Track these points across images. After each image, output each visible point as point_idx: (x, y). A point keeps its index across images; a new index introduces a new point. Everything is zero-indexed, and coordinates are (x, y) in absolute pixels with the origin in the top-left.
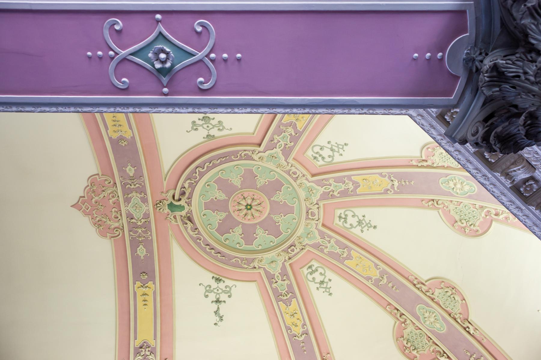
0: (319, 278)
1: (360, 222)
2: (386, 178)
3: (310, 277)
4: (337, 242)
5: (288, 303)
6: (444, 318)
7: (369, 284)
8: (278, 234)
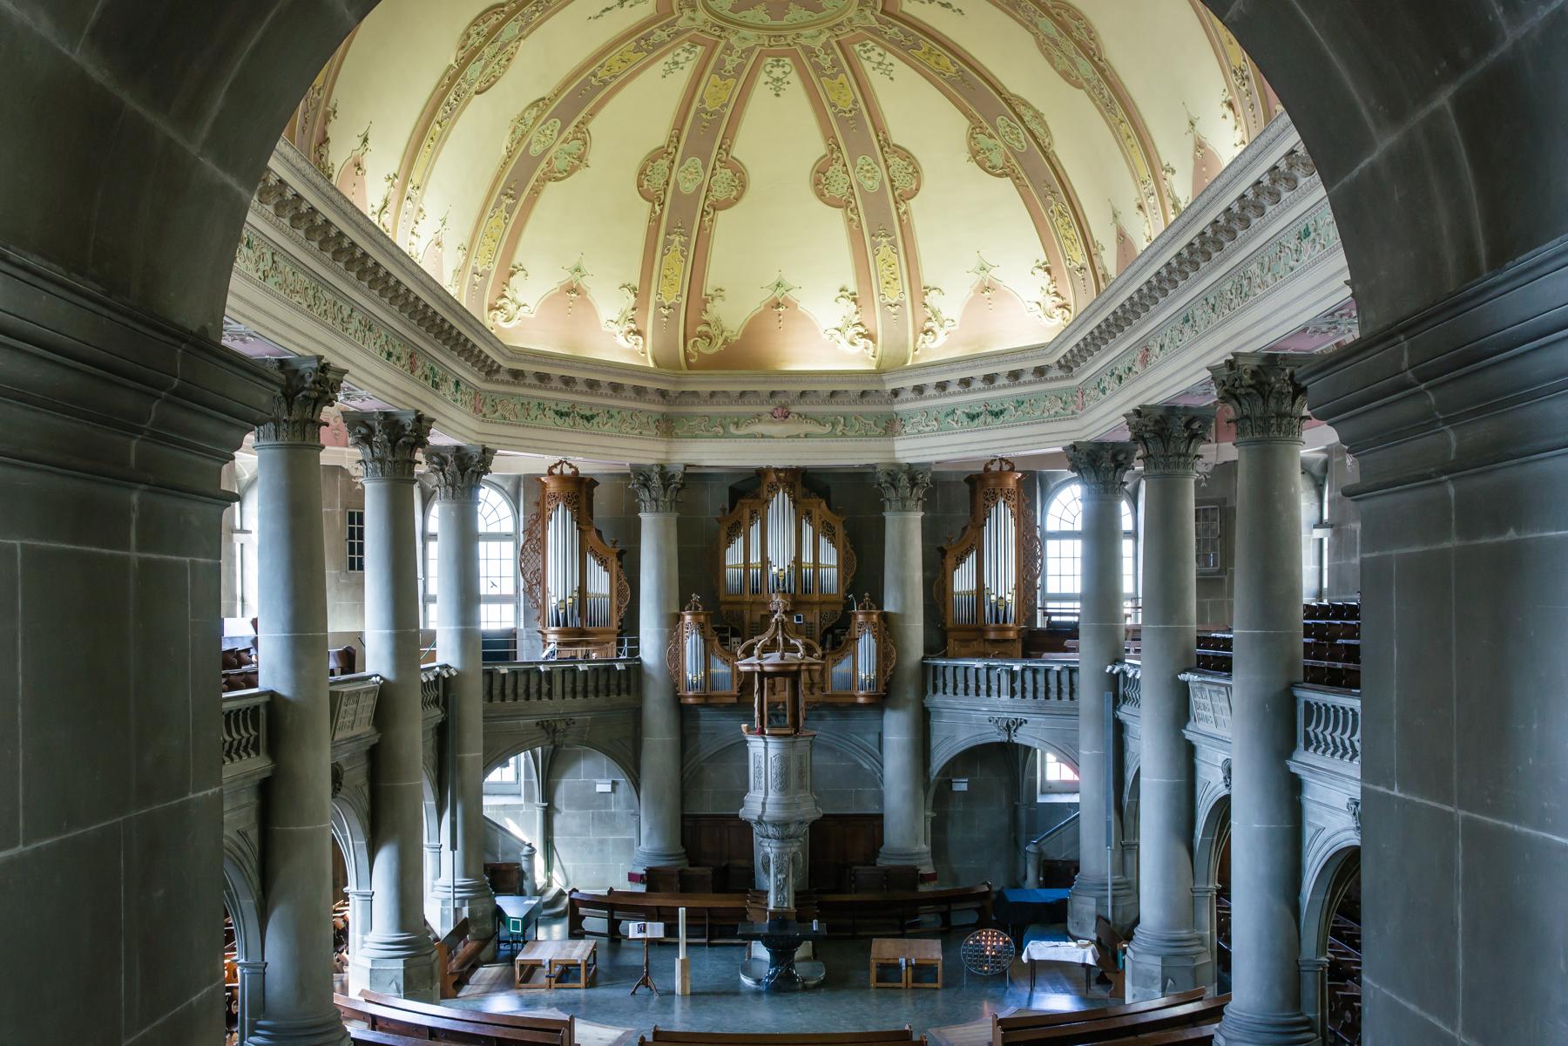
0: (681, 59)
1: (778, 80)
5: (638, 49)
6: (700, 187)
7: (696, 104)
8: (734, 10)
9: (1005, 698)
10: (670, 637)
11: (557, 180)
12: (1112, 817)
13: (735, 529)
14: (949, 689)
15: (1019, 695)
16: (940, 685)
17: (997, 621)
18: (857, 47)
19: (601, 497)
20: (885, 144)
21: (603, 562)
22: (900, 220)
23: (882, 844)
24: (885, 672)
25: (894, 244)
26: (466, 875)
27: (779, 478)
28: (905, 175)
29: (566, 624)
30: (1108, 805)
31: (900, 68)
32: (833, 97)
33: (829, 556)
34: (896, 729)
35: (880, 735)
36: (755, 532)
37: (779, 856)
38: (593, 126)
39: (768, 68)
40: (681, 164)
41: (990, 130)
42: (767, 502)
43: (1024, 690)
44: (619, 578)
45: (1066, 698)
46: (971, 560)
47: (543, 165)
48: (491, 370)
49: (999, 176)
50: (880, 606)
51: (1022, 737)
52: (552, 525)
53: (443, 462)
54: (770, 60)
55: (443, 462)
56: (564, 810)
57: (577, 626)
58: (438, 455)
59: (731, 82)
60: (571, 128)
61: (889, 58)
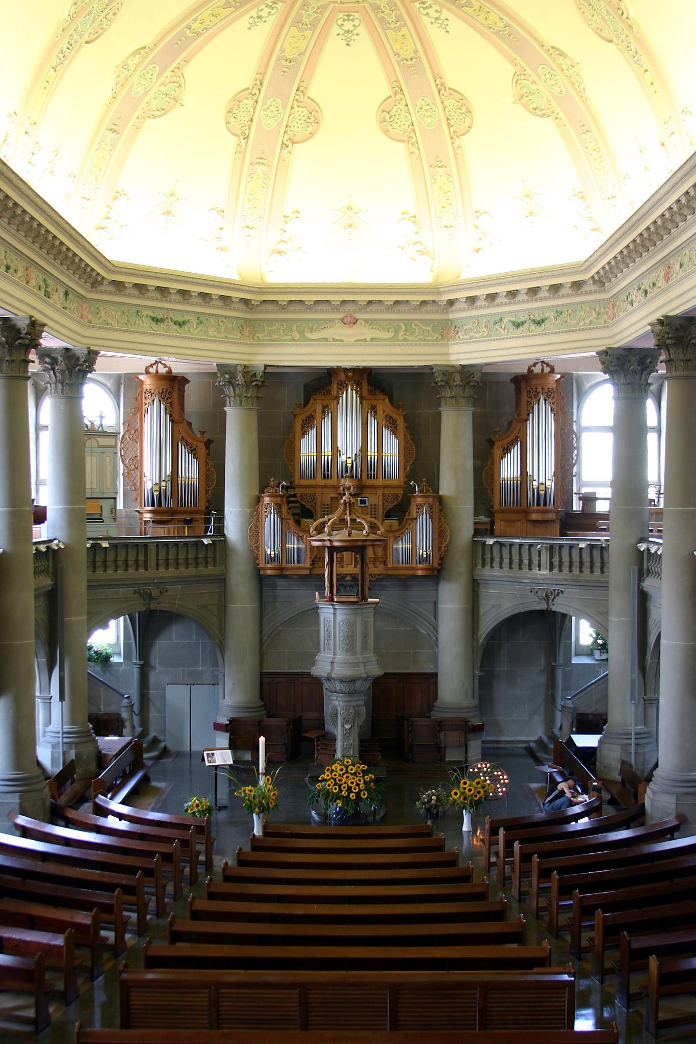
0: (264, 14)
1: (348, 32)
2: (412, 55)
3: (263, 7)
4: (317, 20)
7: (277, 52)
9: (545, 572)
10: (251, 515)
11: (155, 117)
12: (636, 675)
13: (308, 423)
14: (496, 564)
15: (557, 569)
16: (488, 560)
17: (538, 504)
18: (417, 5)
19: (192, 393)
20: (441, 88)
21: (193, 451)
22: (456, 154)
23: (436, 698)
24: (440, 548)
25: (449, 175)
26: (73, 722)
27: (347, 377)
28: (459, 112)
29: (160, 505)
30: (632, 665)
31: (455, 23)
32: (397, 47)
33: (392, 449)
34: (450, 600)
35: (435, 604)
36: (326, 425)
37: (346, 708)
38: (188, 71)
39: (340, 22)
40: (264, 103)
41: (533, 77)
42: (337, 398)
43: (561, 563)
44: (207, 464)
45: (597, 571)
46: (516, 450)
47: (144, 104)
48: (95, 282)
49: (543, 116)
50: (436, 490)
51: (559, 606)
52: (148, 417)
53: (54, 361)
54: (341, 15)
55: (54, 361)
56: (158, 668)
57: (169, 506)
58: (49, 356)
59: (308, 33)
60: (168, 73)
61: (446, 14)
